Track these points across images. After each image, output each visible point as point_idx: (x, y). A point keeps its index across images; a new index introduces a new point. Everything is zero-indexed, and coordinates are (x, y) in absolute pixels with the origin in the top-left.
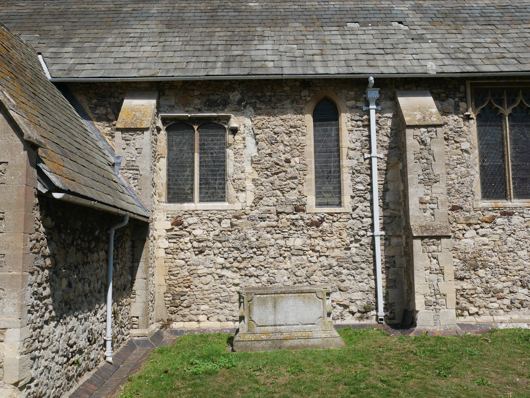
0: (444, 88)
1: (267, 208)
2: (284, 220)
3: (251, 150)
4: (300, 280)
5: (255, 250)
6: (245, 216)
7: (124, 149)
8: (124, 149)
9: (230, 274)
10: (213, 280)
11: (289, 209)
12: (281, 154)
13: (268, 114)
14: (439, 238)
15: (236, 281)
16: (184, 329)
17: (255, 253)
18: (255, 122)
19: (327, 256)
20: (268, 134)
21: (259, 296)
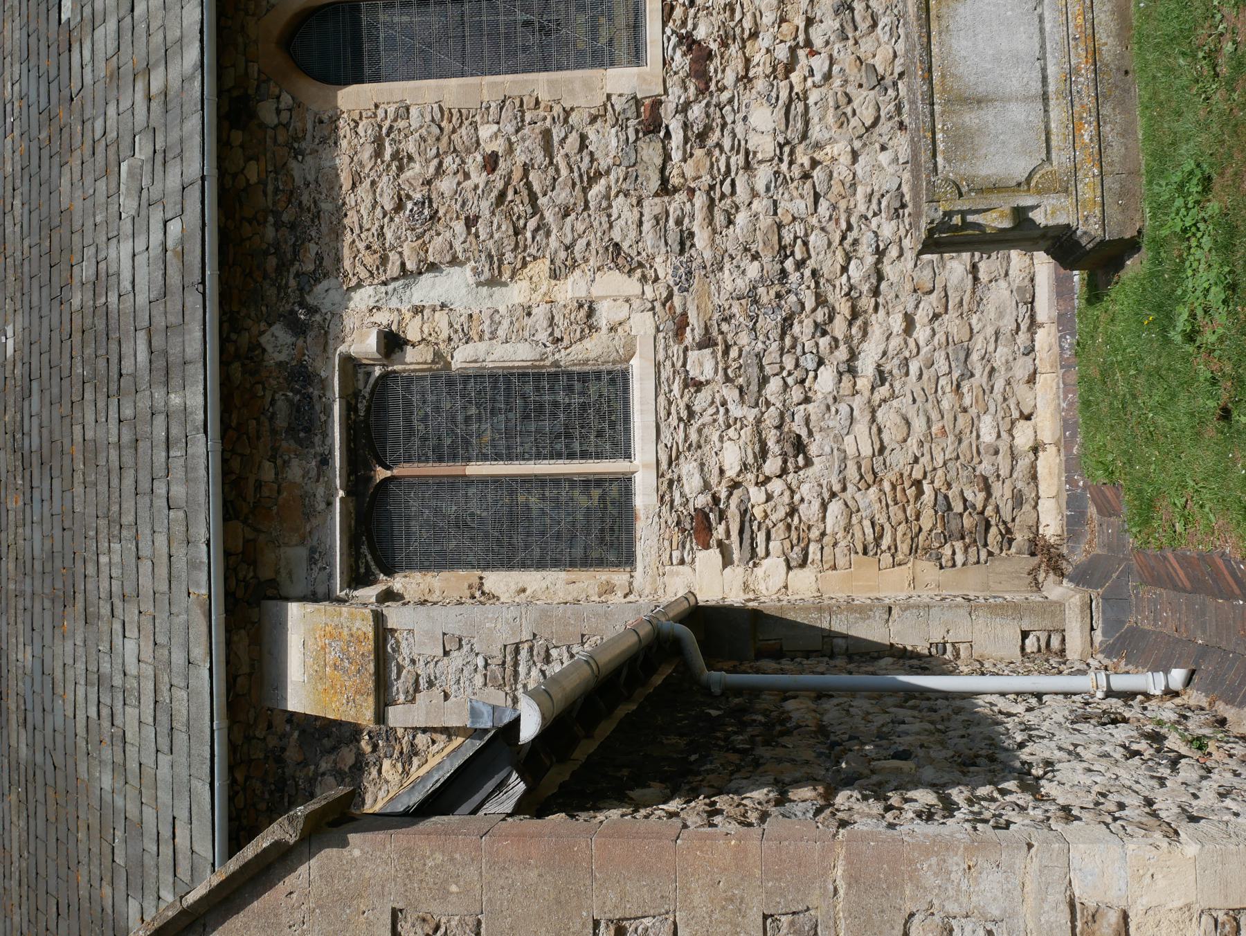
1: (647, 226)
2: (689, 170)
3: (454, 286)
4: (892, 107)
5: (789, 264)
6: (677, 301)
7: (446, 697)
8: (446, 697)
9: (873, 345)
10: (895, 403)
11: (650, 152)
12: (468, 184)
13: (337, 231)
15: (897, 323)
16: (1064, 496)
17: (800, 265)
18: (364, 274)
19: (809, 22)
20: (402, 231)
21: (940, 159)
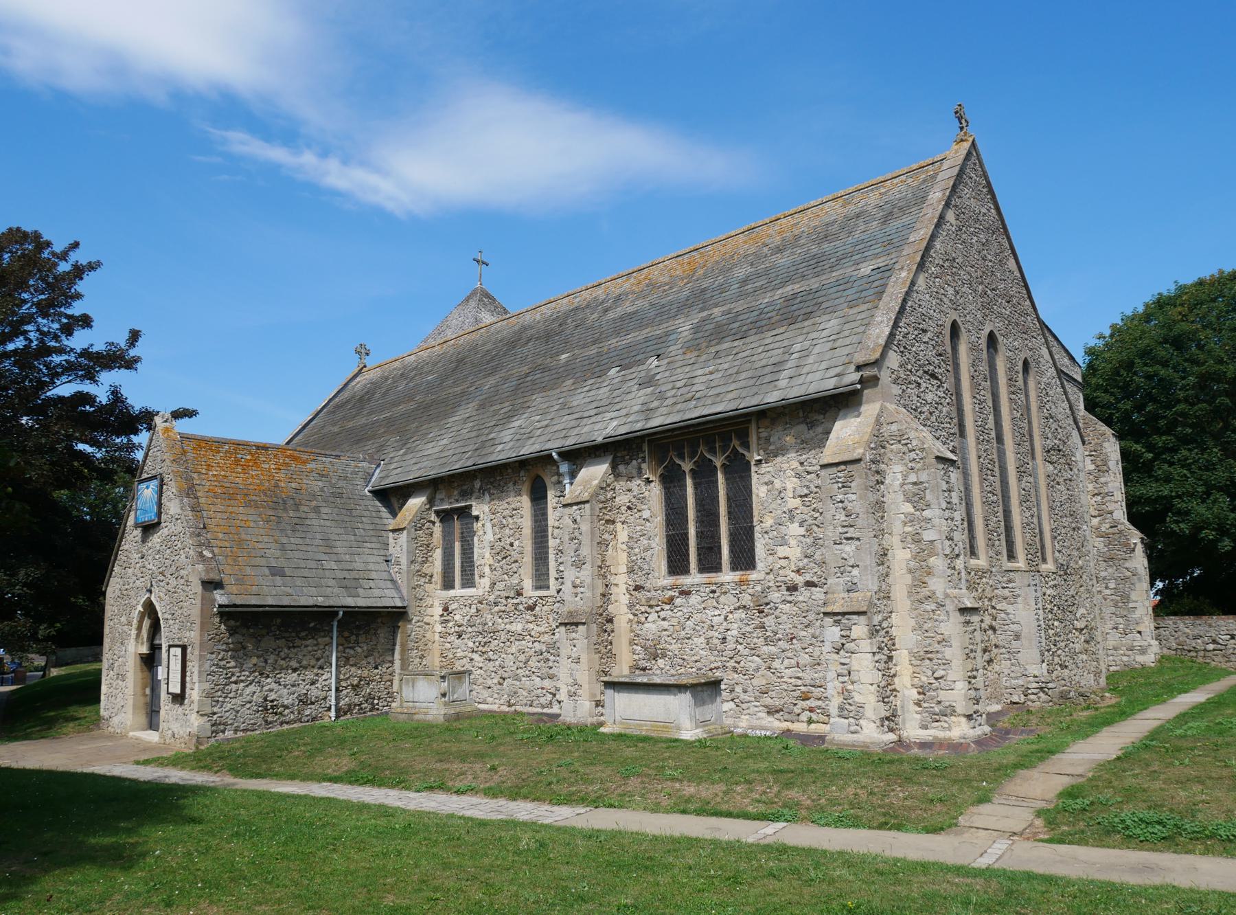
0: (621, 451)
11: (512, 594)
14: (577, 624)
